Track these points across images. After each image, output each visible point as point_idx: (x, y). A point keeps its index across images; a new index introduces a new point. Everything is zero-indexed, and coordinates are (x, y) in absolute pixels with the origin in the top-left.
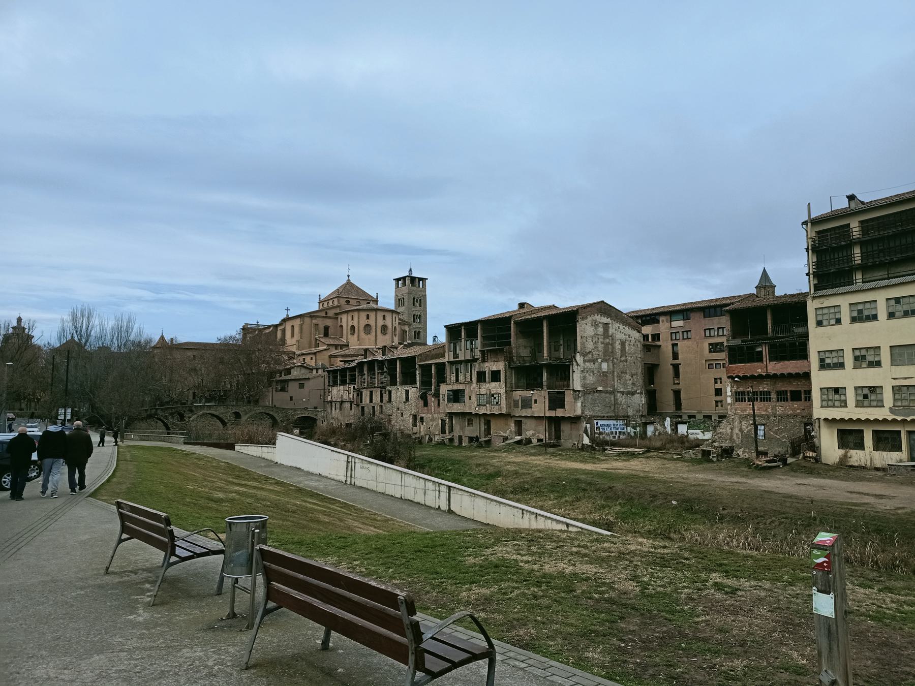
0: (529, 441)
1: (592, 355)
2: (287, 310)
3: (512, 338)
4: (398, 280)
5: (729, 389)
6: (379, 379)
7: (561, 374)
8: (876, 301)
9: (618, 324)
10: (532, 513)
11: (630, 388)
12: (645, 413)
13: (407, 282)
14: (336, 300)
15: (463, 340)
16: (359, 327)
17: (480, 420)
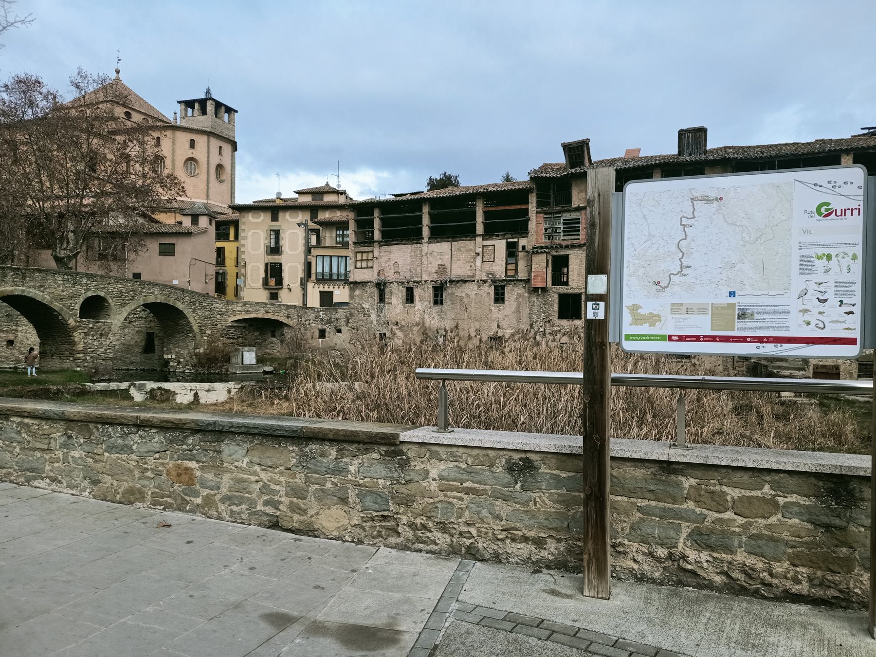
4: (189, 104)
16: (173, 161)
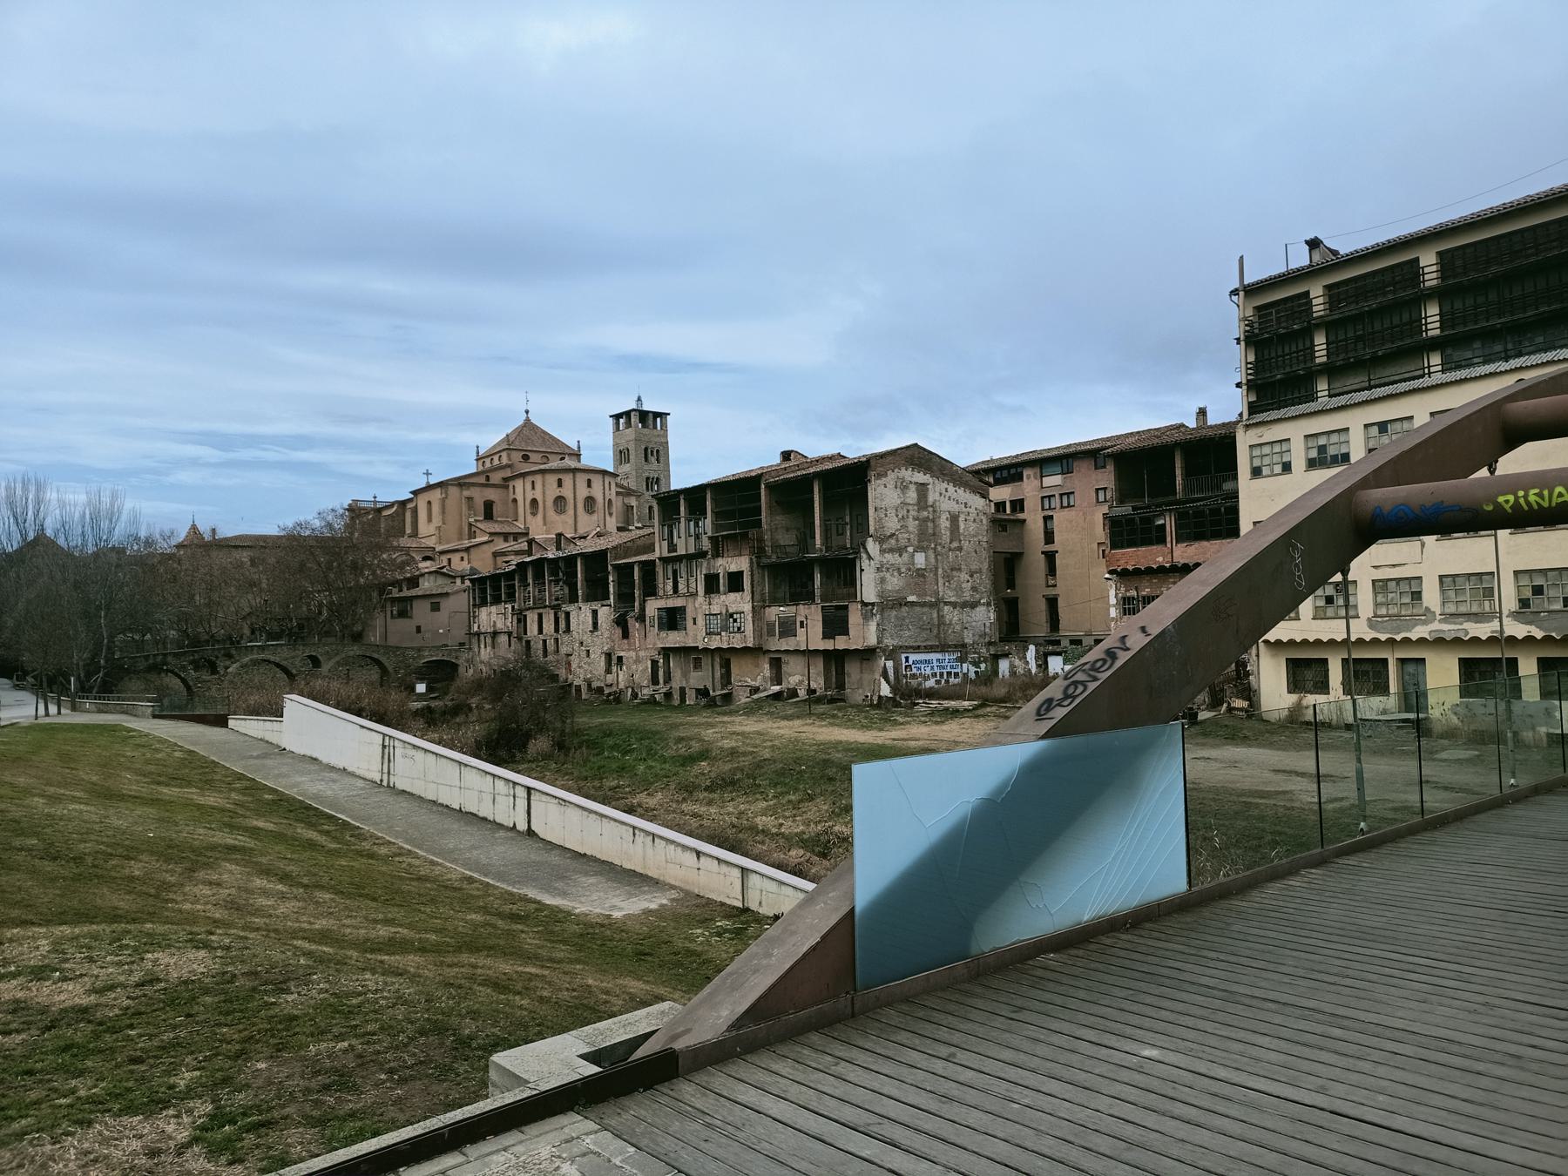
0: (793, 693)
1: (897, 540)
2: (427, 474)
3: (763, 514)
4: (617, 417)
5: (1112, 593)
6: (553, 591)
7: (845, 576)
8: (1347, 429)
9: (945, 485)
10: (647, 833)
11: (967, 596)
12: (995, 638)
13: (632, 420)
14: (504, 454)
15: (682, 519)
16: (544, 502)
17: (713, 660)
